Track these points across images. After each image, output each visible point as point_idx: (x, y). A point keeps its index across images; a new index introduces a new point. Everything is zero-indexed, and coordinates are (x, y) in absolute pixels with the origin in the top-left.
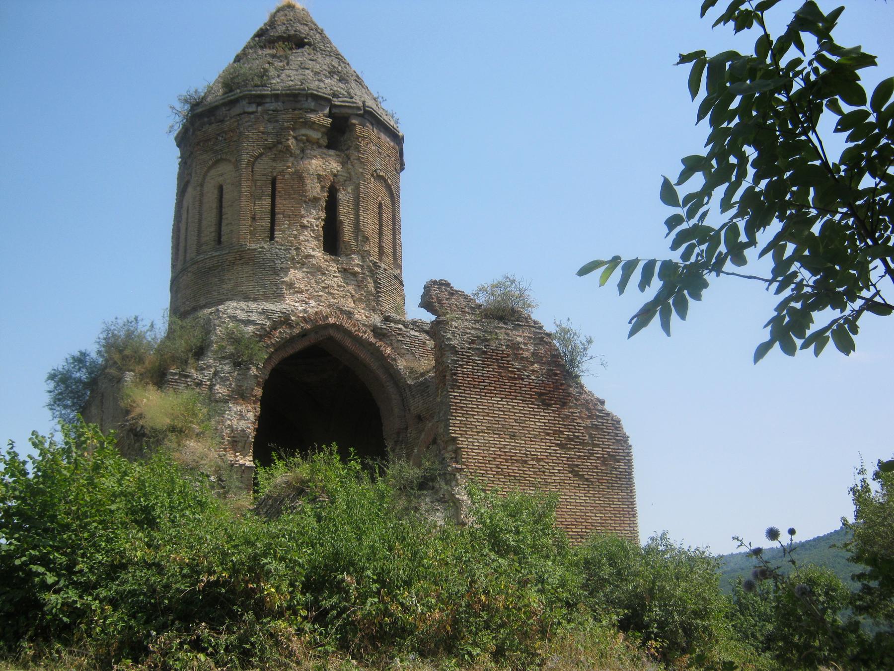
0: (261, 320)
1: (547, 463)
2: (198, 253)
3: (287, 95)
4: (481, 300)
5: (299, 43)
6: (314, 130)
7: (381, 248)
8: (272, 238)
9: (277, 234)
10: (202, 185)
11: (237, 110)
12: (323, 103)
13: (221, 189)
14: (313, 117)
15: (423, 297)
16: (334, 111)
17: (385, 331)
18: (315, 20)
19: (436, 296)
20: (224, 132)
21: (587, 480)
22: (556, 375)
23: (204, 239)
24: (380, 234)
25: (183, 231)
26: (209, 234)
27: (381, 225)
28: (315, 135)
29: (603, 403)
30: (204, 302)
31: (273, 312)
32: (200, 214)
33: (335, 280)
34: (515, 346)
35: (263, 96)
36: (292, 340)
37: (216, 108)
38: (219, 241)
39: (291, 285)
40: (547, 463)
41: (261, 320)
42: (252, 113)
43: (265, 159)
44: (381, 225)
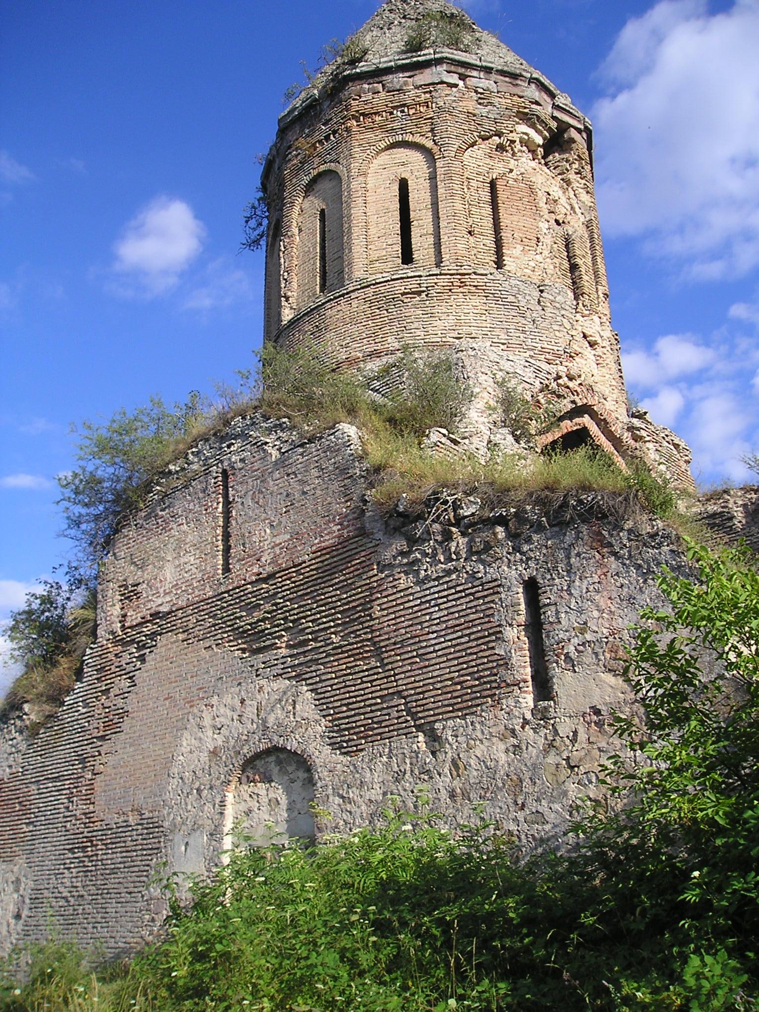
0: (529, 374)
3: (502, 73)
6: (537, 131)
8: (499, 264)
9: (507, 260)
11: (425, 77)
17: (644, 433)
20: (404, 105)
30: (397, 345)
37: (388, 71)
41: (529, 374)
42: (456, 86)
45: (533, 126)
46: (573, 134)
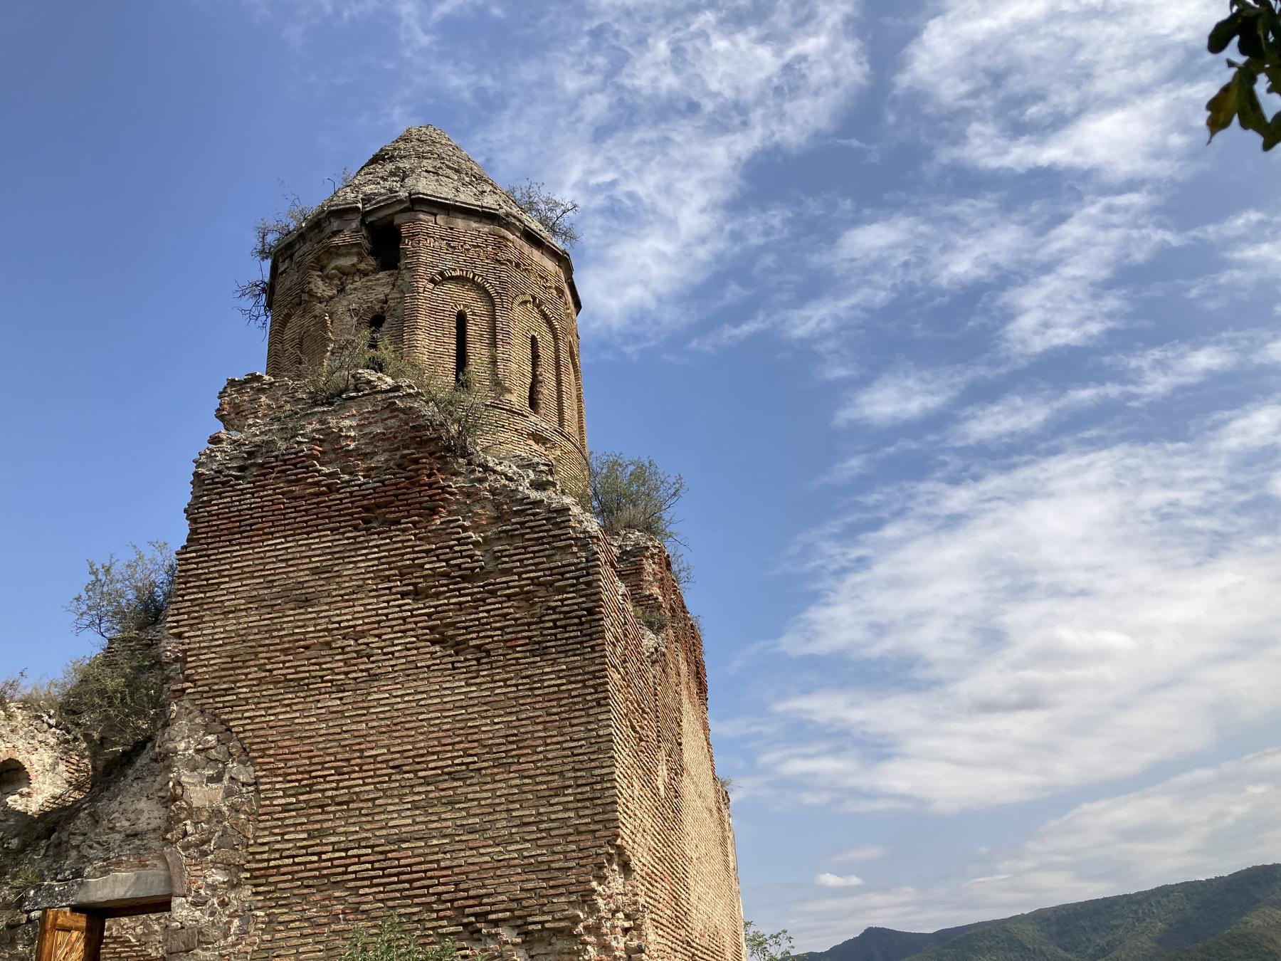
1: (379, 636)
6: (345, 255)
12: (350, 217)
14: (337, 240)
16: (370, 219)
21: (478, 647)
22: (416, 461)
28: (346, 262)
40: (379, 636)
43: (294, 319)
45: (339, 255)
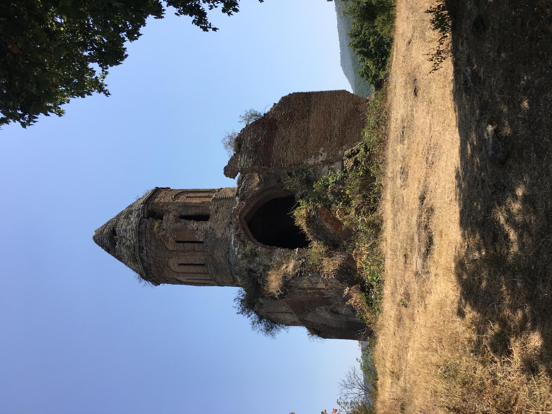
2: (208, 274)
3: (139, 236)
4: (232, 153)
5: (113, 232)
7: (206, 197)
8: (202, 242)
10: (178, 273)
11: (145, 258)
13: (180, 265)
14: (148, 226)
15: (231, 178)
16: (146, 216)
18: (101, 226)
19: (229, 171)
22: (264, 123)
23: (202, 271)
24: (200, 197)
25: (197, 281)
26: (200, 269)
27: (196, 197)
28: (157, 224)
29: (275, 104)
31: (234, 241)
32: (191, 273)
33: (219, 216)
34: (252, 139)
35: (139, 247)
36: (246, 234)
37: (144, 267)
38: (203, 265)
39: (223, 234)
44: (196, 197)
45: (153, 226)
46: (150, 208)
